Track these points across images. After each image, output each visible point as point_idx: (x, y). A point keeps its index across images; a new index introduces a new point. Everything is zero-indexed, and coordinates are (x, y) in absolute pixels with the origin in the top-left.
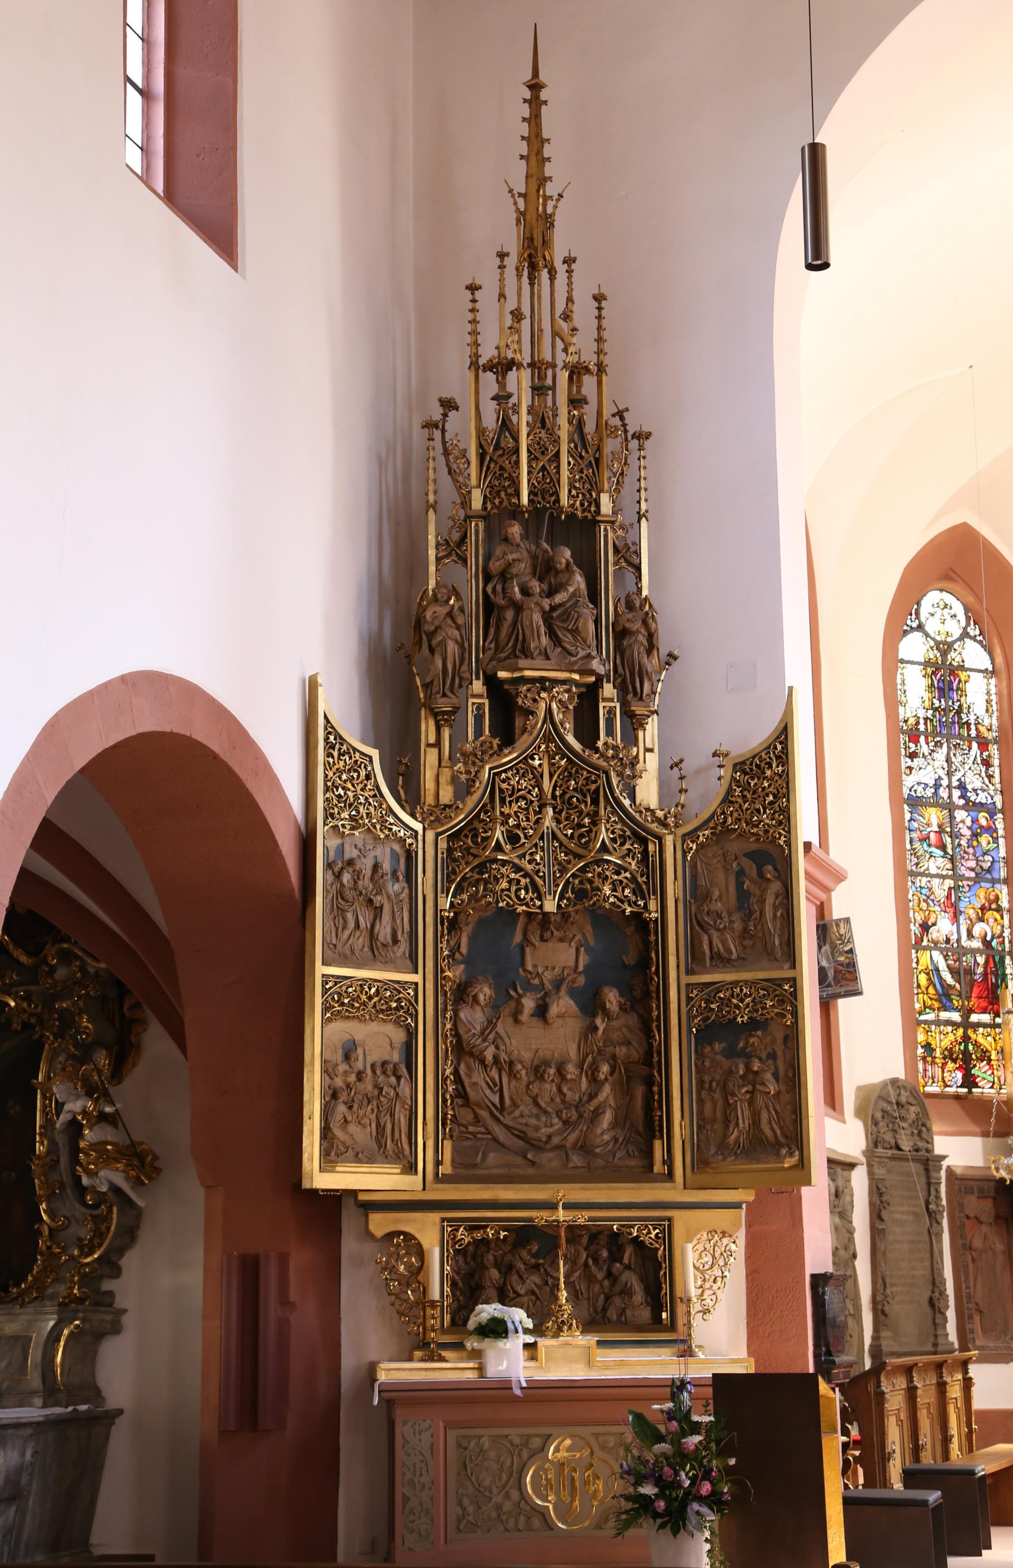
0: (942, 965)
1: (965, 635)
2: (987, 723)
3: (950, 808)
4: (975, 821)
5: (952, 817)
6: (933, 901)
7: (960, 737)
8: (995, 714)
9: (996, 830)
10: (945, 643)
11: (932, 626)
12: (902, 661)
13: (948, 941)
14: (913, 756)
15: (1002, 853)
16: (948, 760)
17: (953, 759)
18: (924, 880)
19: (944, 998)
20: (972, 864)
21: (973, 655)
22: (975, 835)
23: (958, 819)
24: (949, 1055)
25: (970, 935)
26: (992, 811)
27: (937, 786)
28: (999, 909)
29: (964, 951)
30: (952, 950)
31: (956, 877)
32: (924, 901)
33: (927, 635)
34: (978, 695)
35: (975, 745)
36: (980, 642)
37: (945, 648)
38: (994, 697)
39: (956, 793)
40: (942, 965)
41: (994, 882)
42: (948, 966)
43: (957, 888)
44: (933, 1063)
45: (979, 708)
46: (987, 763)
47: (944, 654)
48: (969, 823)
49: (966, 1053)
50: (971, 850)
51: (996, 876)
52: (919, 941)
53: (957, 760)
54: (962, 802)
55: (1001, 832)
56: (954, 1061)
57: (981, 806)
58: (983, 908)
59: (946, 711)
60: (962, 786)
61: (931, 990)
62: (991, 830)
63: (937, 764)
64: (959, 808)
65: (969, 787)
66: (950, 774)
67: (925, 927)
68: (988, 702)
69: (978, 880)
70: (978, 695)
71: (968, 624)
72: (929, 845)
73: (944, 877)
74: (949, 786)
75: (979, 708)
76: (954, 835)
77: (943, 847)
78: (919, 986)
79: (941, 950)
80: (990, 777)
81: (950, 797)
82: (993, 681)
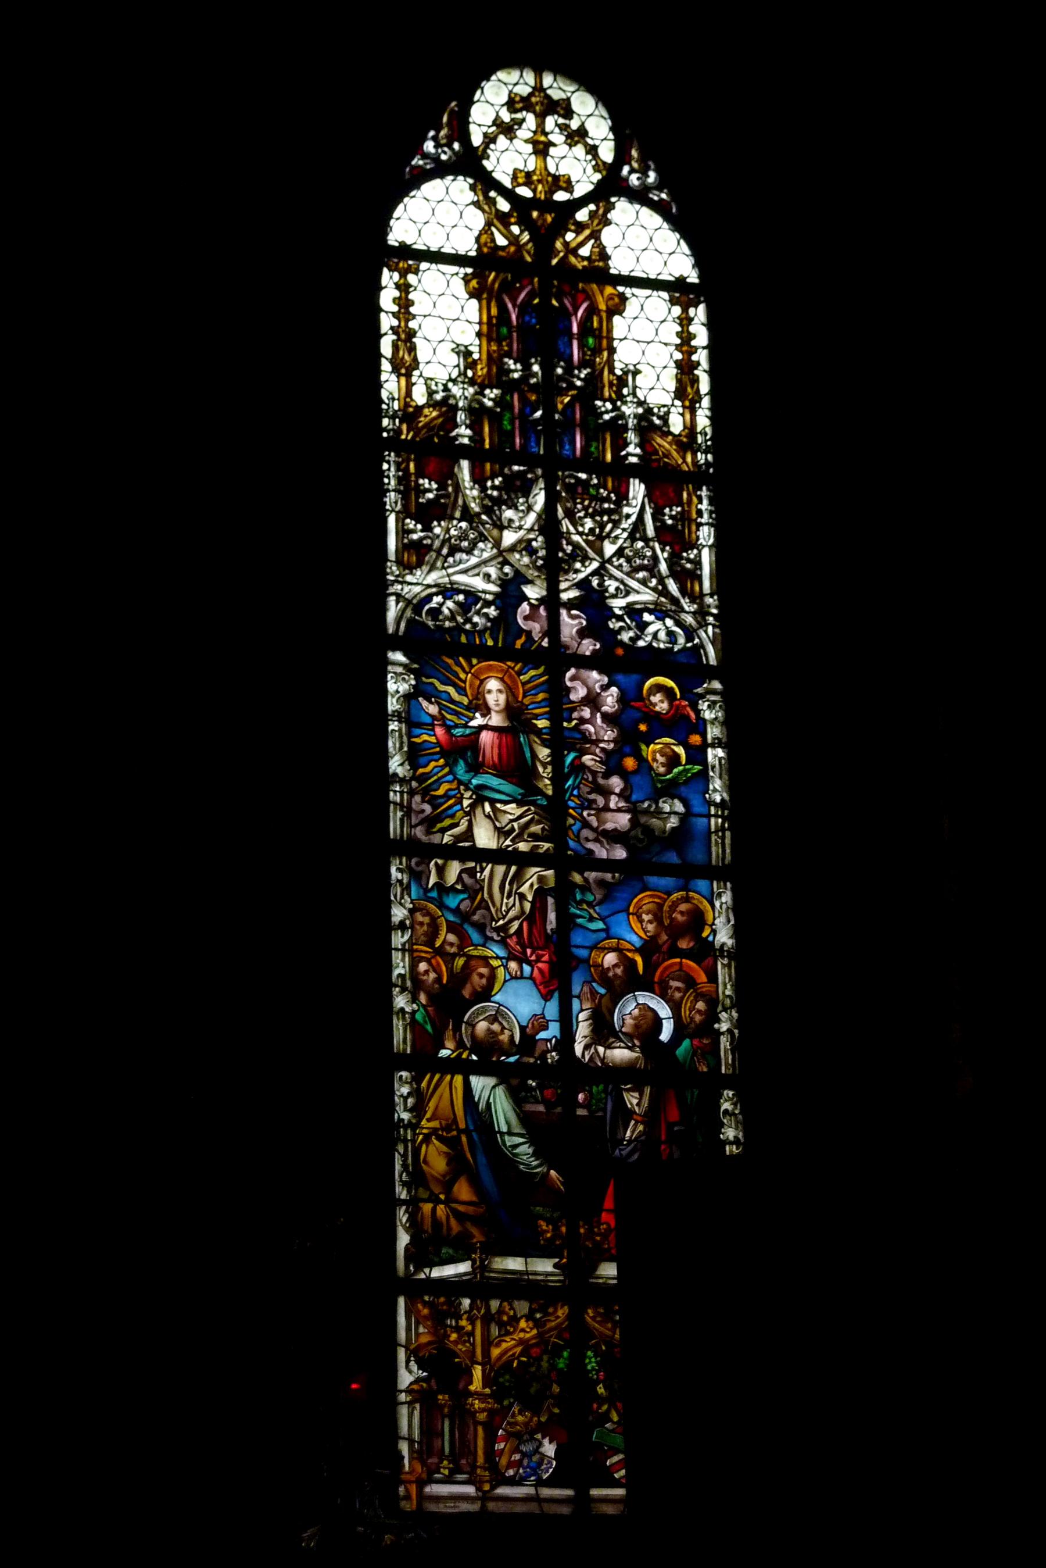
0: (503, 1111)
1: (610, 187)
2: (676, 424)
3: (557, 659)
4: (629, 698)
5: (557, 693)
6: (481, 928)
7: (590, 463)
8: (706, 402)
9: (700, 726)
10: (547, 205)
11: (507, 160)
12: (405, 251)
13: (528, 1041)
14: (428, 514)
15: (717, 789)
16: (548, 524)
17: (566, 525)
18: (454, 869)
19: (507, 1212)
20: (622, 821)
21: (642, 242)
22: (630, 740)
23: (579, 693)
24: (512, 1382)
25: (604, 1031)
26: (686, 667)
27: (510, 592)
28: (705, 952)
29: (572, 1072)
30: (534, 1070)
31: (564, 860)
32: (451, 928)
33: (484, 182)
34: (651, 347)
35: (637, 490)
36: (658, 208)
37: (543, 212)
38: (702, 357)
39: (570, 624)
40: (503, 1111)
41: (688, 873)
42: (525, 1118)
43: (564, 892)
44: (462, 1415)
45: (656, 386)
46: (676, 537)
47: (544, 239)
48: (610, 700)
49: (576, 1378)
50: (616, 783)
51: (697, 855)
52: (425, 1044)
53: (576, 532)
54: (588, 647)
55: (713, 732)
56: (532, 1405)
57: (655, 660)
58: (648, 948)
59: (550, 388)
60: (593, 601)
61: (463, 1191)
62: (682, 725)
63: (509, 538)
64: (585, 663)
65: (617, 604)
66: (553, 569)
67: (452, 1000)
68: (686, 369)
69: (633, 873)
70: (651, 347)
71: (621, 156)
72: (476, 768)
73: (524, 861)
74: (552, 602)
75: (656, 386)
76: (565, 740)
77: (517, 769)
78: (417, 1177)
79: (503, 1075)
80: (687, 577)
81: (553, 628)
82: (699, 313)
